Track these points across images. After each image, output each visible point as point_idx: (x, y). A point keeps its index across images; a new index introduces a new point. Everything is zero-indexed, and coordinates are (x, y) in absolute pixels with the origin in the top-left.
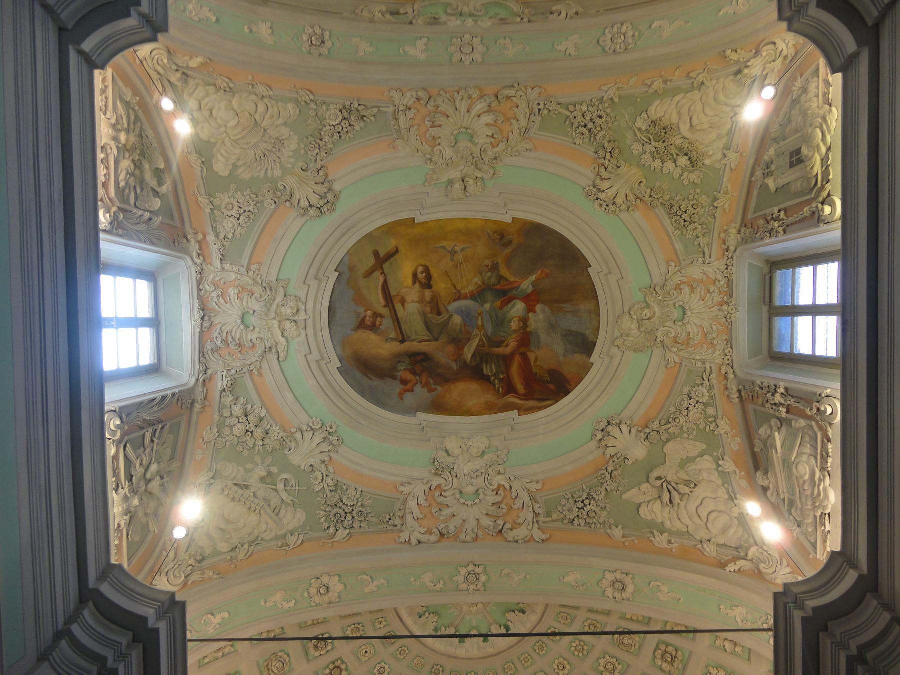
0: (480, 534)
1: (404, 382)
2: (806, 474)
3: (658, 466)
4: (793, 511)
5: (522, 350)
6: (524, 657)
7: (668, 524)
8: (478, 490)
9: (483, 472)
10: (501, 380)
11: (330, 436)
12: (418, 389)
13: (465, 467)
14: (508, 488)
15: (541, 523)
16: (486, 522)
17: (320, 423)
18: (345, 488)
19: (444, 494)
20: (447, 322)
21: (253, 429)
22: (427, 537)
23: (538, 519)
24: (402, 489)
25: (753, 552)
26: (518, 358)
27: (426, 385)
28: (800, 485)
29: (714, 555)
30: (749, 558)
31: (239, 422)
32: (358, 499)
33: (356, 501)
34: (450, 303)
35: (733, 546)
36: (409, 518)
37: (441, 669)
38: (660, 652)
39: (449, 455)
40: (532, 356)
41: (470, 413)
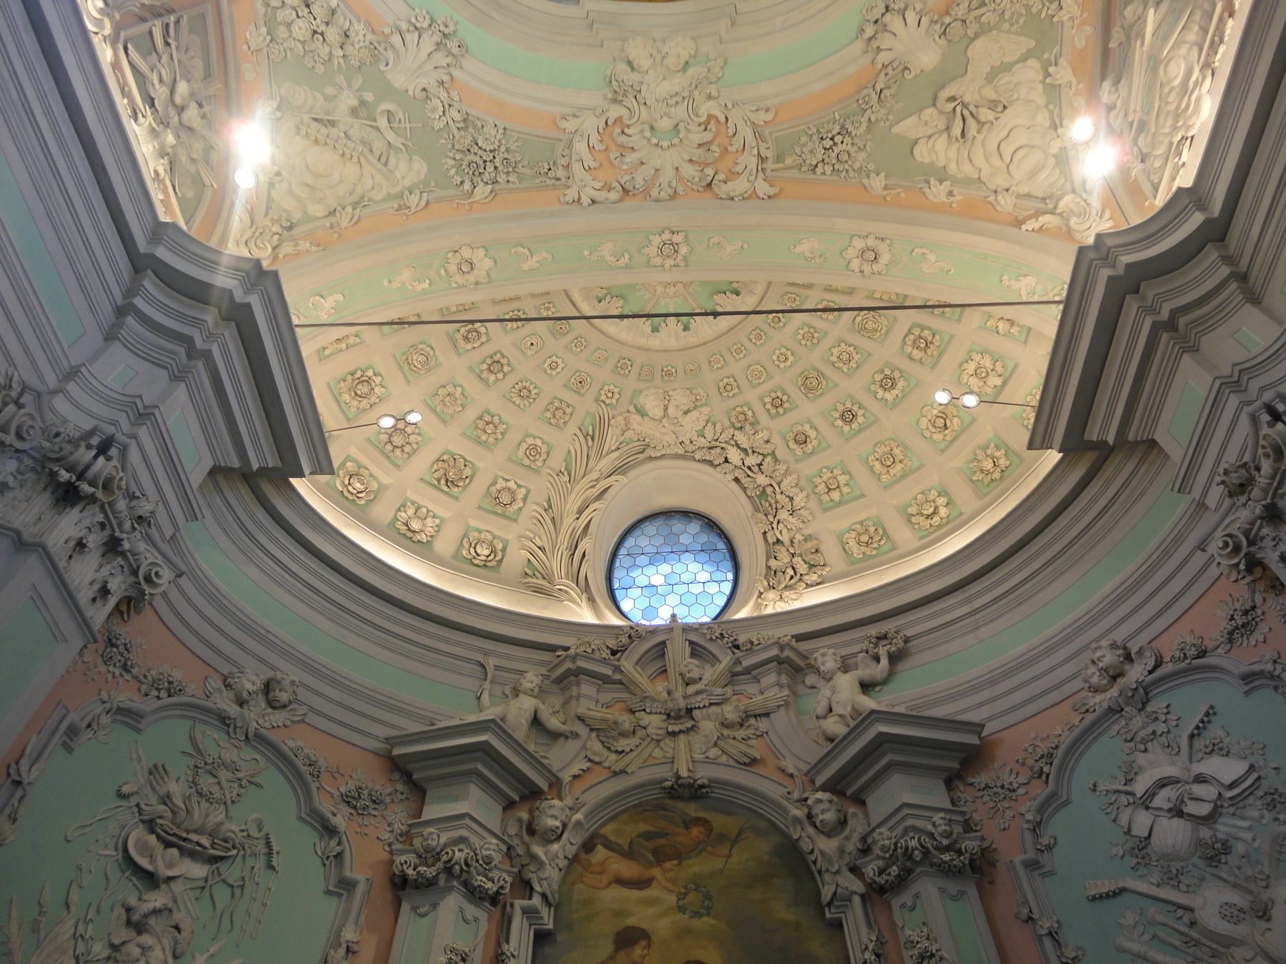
0: (680, 189)
2: (1175, 78)
4: (1141, 139)
6: (735, 347)
7: (953, 168)
8: (677, 125)
9: (685, 94)
13: (658, 88)
14: (722, 119)
15: (768, 172)
16: (689, 171)
17: (428, 17)
18: (479, 124)
19: (626, 131)
21: (323, 28)
22: (604, 194)
23: (765, 166)
24: (563, 124)
25: (1067, 202)
28: (1163, 95)
29: (1010, 208)
30: (1058, 211)
31: (298, 16)
32: (500, 141)
33: (497, 143)
35: (1040, 195)
36: (577, 167)
37: (629, 363)
38: (912, 337)
39: (633, 69)
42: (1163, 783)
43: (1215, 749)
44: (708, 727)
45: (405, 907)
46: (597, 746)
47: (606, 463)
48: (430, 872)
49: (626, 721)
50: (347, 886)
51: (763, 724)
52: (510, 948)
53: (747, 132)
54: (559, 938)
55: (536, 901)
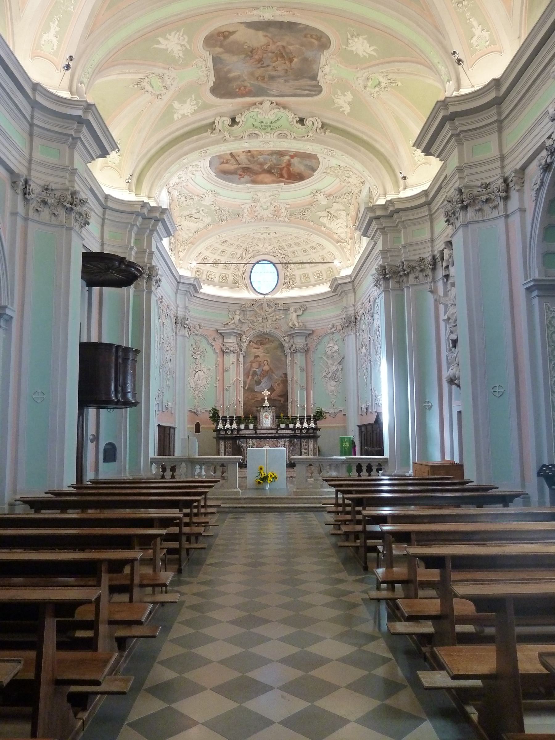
1: (240, 175)
7: (327, 225)
11: (215, 194)
12: (246, 177)
16: (270, 215)
22: (251, 220)
24: (241, 206)
26: (285, 169)
27: (249, 175)
36: (245, 215)
40: (291, 169)
41: (266, 183)
44: (270, 321)
47: (250, 256)
49: (255, 320)
51: (279, 321)
52: (240, 359)
55: (243, 352)
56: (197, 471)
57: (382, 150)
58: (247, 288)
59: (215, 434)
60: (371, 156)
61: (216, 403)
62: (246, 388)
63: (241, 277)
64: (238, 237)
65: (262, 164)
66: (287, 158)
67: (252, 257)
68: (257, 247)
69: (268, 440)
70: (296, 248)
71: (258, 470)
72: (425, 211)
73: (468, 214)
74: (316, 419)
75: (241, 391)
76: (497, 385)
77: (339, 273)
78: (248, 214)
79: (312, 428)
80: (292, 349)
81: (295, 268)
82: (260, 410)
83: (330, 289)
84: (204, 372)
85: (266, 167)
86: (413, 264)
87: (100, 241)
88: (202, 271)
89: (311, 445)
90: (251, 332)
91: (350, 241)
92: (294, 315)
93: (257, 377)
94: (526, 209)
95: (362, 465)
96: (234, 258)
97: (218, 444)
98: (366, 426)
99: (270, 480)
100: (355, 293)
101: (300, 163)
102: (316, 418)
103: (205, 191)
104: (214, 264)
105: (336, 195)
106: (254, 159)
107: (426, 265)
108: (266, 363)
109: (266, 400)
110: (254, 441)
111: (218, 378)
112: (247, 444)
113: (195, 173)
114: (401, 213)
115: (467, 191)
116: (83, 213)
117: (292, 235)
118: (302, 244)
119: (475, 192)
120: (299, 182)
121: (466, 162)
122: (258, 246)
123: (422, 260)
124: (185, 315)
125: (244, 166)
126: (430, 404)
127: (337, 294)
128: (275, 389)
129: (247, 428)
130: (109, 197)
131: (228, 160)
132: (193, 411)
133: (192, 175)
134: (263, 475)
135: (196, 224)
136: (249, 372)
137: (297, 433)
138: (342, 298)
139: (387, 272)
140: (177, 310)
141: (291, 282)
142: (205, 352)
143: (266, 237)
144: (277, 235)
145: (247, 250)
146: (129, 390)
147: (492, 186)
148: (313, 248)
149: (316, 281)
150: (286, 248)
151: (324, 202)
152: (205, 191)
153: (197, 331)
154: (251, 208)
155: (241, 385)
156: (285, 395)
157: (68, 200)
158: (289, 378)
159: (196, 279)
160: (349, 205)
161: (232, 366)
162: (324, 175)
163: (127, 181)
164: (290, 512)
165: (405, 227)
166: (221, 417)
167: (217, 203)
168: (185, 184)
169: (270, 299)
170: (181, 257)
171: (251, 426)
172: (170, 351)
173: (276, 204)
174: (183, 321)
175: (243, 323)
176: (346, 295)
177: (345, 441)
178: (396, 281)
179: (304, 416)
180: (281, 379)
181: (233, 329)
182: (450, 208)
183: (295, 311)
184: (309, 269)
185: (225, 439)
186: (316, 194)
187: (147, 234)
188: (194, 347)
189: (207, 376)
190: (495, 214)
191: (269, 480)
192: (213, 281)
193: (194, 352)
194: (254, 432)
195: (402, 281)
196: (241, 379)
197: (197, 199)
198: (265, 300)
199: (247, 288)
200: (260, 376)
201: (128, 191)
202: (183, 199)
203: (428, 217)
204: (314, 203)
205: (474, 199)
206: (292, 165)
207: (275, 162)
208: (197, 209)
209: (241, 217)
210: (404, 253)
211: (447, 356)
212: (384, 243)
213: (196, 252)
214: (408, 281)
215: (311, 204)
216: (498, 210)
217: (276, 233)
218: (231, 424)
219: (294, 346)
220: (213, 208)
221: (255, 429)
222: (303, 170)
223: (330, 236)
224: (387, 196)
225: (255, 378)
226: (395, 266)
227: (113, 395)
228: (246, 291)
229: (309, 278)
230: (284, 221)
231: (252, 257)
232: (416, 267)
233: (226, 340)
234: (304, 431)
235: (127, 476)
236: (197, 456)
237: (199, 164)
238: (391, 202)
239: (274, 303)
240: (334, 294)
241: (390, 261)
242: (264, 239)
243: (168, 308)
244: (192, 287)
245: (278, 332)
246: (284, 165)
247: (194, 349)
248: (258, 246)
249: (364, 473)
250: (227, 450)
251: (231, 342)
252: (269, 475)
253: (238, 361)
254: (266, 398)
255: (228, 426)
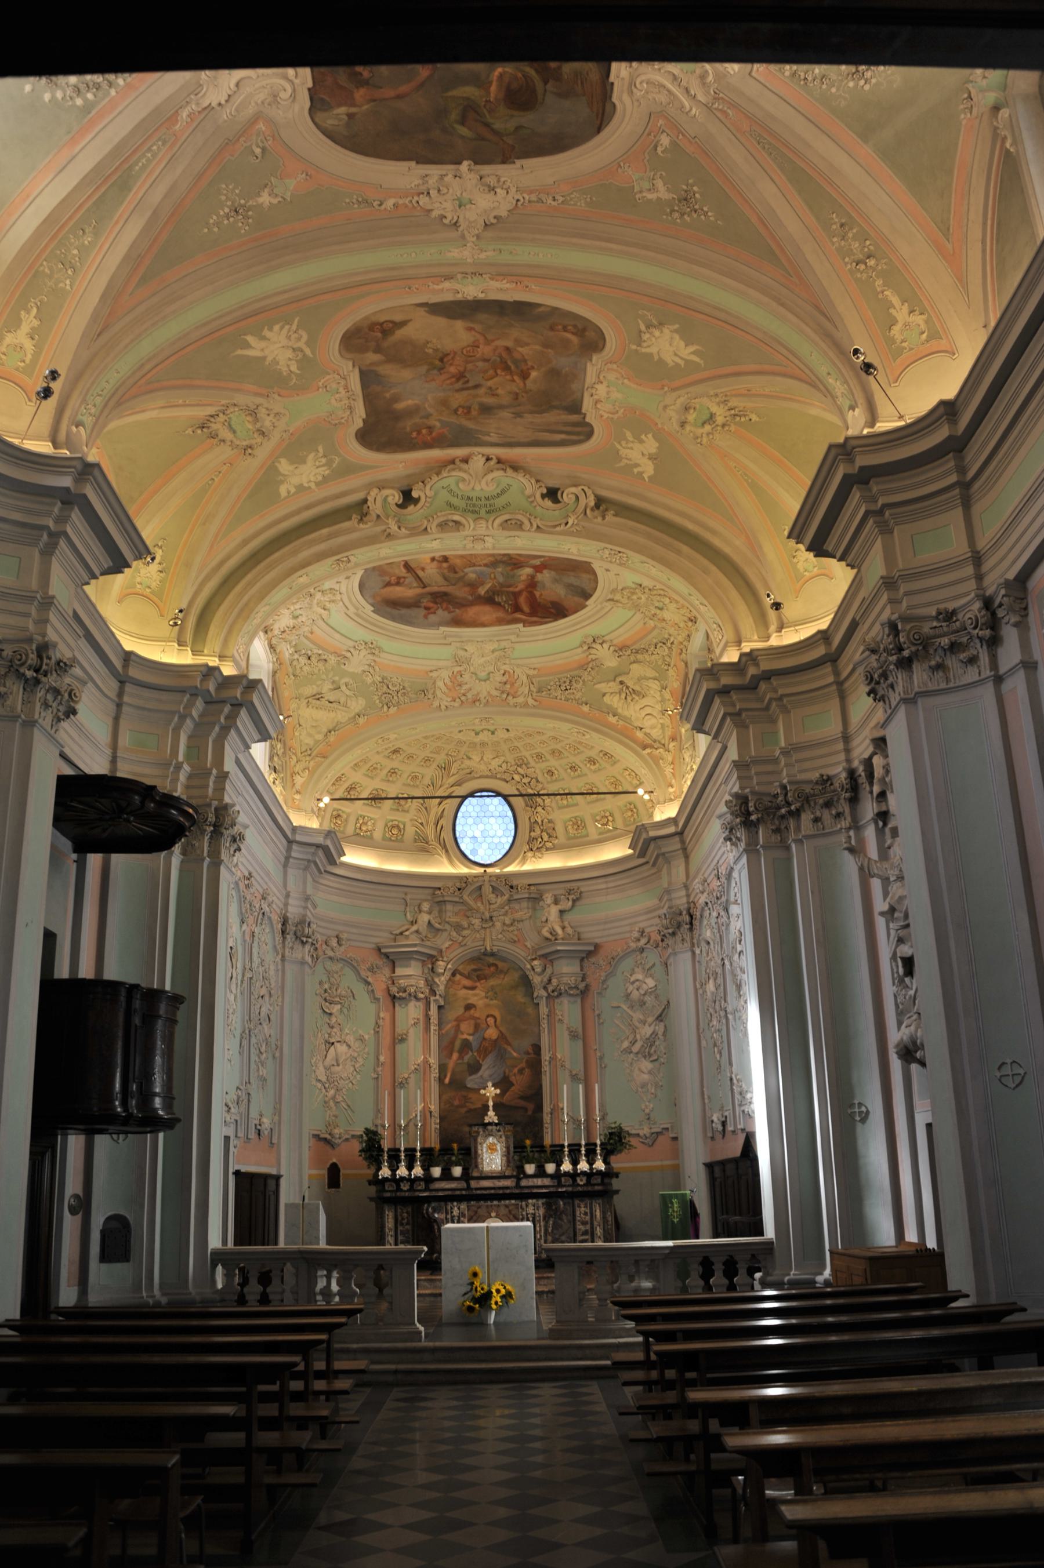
1: (427, 608)
3: (624, 674)
5: (529, 589)
7: (620, 711)
10: (509, 605)
11: (373, 648)
12: (440, 612)
13: (477, 661)
16: (495, 693)
20: (464, 576)
22: (452, 703)
24: (431, 674)
26: (525, 594)
27: (447, 609)
34: (465, 568)
36: (438, 693)
40: (537, 594)
41: (483, 625)
42: (637, 980)
43: (652, 976)
44: (498, 925)
45: (397, 1005)
46: (454, 934)
47: (452, 780)
48: (404, 995)
49: (465, 924)
50: (378, 1000)
51: (520, 925)
53: (525, 679)
54: (446, 1007)
55: (438, 997)
56: (321, 1284)
57: (727, 550)
58: (447, 851)
59: (372, 1190)
60: (705, 562)
61: (377, 1117)
62: (447, 1081)
63: (434, 827)
64: (425, 741)
65: (473, 586)
66: (528, 571)
67: (458, 784)
68: (467, 762)
69: (495, 1203)
70: (553, 763)
71: (467, 1278)
72: (825, 676)
73: (915, 676)
74: (608, 1154)
75: (435, 1087)
76: (1009, 1061)
77: (651, 816)
78: (446, 691)
79: (599, 1172)
80: (550, 988)
81: (554, 805)
82: (478, 1133)
83: (631, 851)
84: (349, 1046)
85: (482, 591)
86: (808, 789)
87: (109, 752)
88: (345, 816)
89: (598, 1213)
90: (457, 952)
91: (672, 745)
92: (554, 911)
93: (470, 1053)
94: (1036, 663)
95: (713, 1259)
96: (417, 786)
97: (381, 1215)
98: (723, 1163)
99: (496, 1303)
100: (687, 857)
101: (556, 581)
102: (609, 1147)
103: (351, 643)
104: (371, 799)
105: (636, 647)
106: (457, 576)
107: (835, 791)
108: (491, 1021)
109: (491, 1108)
110: (463, 1206)
111: (382, 1059)
112: (447, 1213)
113: (328, 605)
114: (774, 681)
115: (908, 627)
116: (62, 690)
117: (543, 734)
118: (566, 754)
119: (926, 629)
120: (556, 620)
121: (901, 567)
122: (469, 758)
123: (826, 781)
124: (305, 916)
125: (436, 589)
126: (863, 1109)
127: (647, 863)
128: (515, 1082)
129: (447, 1175)
130: (133, 657)
131: (399, 578)
132: (322, 1136)
133: (323, 611)
134: (479, 1289)
135: (332, 715)
136: (452, 1043)
137: (564, 1186)
138: (660, 871)
139: (751, 809)
140: (286, 905)
141: (545, 837)
142: (351, 999)
143: (486, 740)
144: (511, 734)
145: (445, 768)
146: (157, 1090)
147: (960, 616)
148: (592, 761)
149: (600, 834)
150: (532, 763)
151: (611, 662)
152: (351, 643)
153: (332, 949)
154: (453, 677)
155: (435, 1073)
156: (535, 1095)
157: (29, 662)
158: (546, 1056)
159: (329, 834)
160: (666, 668)
161: (412, 1031)
162: (609, 605)
163: (171, 623)
164: (543, 1380)
165: (785, 710)
166: (386, 1149)
167: (377, 668)
168: (306, 629)
169: (498, 877)
170: (298, 787)
171: (457, 1171)
172: (267, 998)
173: (507, 668)
174: (299, 927)
175: (438, 930)
176: (668, 862)
177: (672, 1203)
178: (774, 827)
179: (580, 1145)
180: (526, 1057)
181: (415, 945)
182: (875, 664)
183: (556, 902)
184: (584, 808)
185: (395, 1201)
186: (594, 645)
187: (214, 735)
188: (326, 986)
189: (356, 1055)
190: (971, 675)
191: (493, 1302)
192: (371, 837)
193: (325, 1000)
194: (463, 1185)
195: (786, 828)
196: (433, 1061)
197: (333, 660)
198: (486, 878)
199: (447, 851)
200: (478, 1051)
201: (176, 645)
202: (303, 660)
203: (834, 687)
204: (590, 665)
205: (925, 645)
206: (538, 585)
207: (501, 579)
208: (334, 682)
209: (430, 696)
210: (786, 765)
211: (895, 996)
212: (742, 745)
213: (332, 774)
214: (798, 829)
215: (583, 667)
216: (979, 667)
217: (508, 730)
218: (410, 1168)
219: (554, 982)
220: (369, 680)
221: (466, 1176)
222: (563, 597)
223: (626, 734)
224: (743, 644)
225: (467, 1058)
226: (769, 794)
227: (117, 1103)
228: (445, 860)
229: (585, 827)
230: (526, 705)
231: (458, 784)
232: (814, 795)
233: (400, 971)
234: (581, 1181)
235: (156, 1294)
236: (323, 1245)
237: (337, 587)
238: (750, 657)
239: (509, 883)
240: (642, 861)
241: (758, 784)
242: (483, 744)
243: (264, 898)
244: (320, 853)
245: (518, 950)
246: (521, 586)
247: (326, 991)
248: (469, 758)
249: (718, 1279)
250: (400, 1228)
251: (411, 974)
252: (494, 1291)
253: (428, 1018)
254: (491, 1103)
255: (402, 1171)
